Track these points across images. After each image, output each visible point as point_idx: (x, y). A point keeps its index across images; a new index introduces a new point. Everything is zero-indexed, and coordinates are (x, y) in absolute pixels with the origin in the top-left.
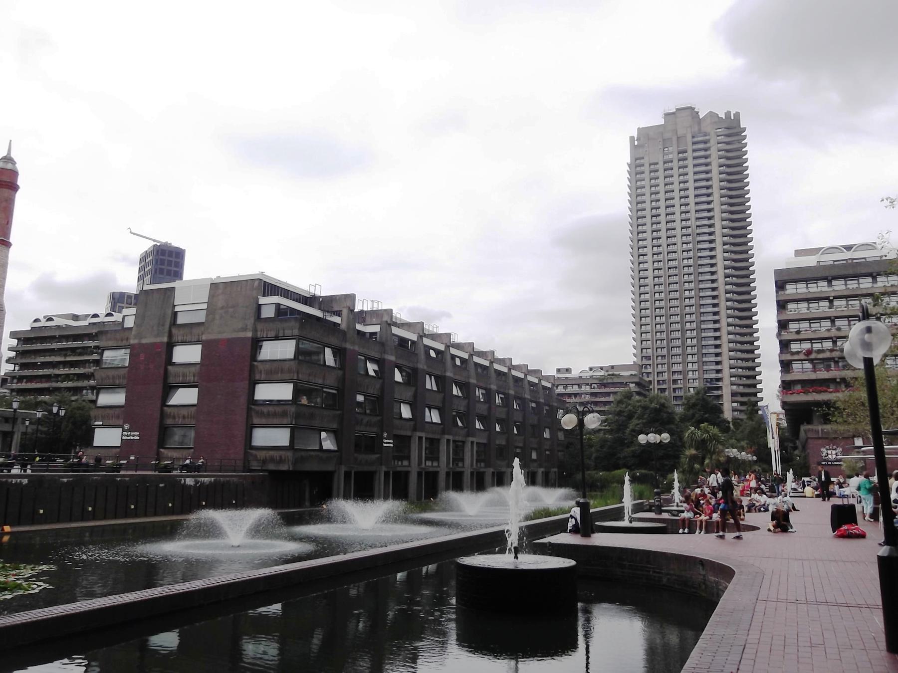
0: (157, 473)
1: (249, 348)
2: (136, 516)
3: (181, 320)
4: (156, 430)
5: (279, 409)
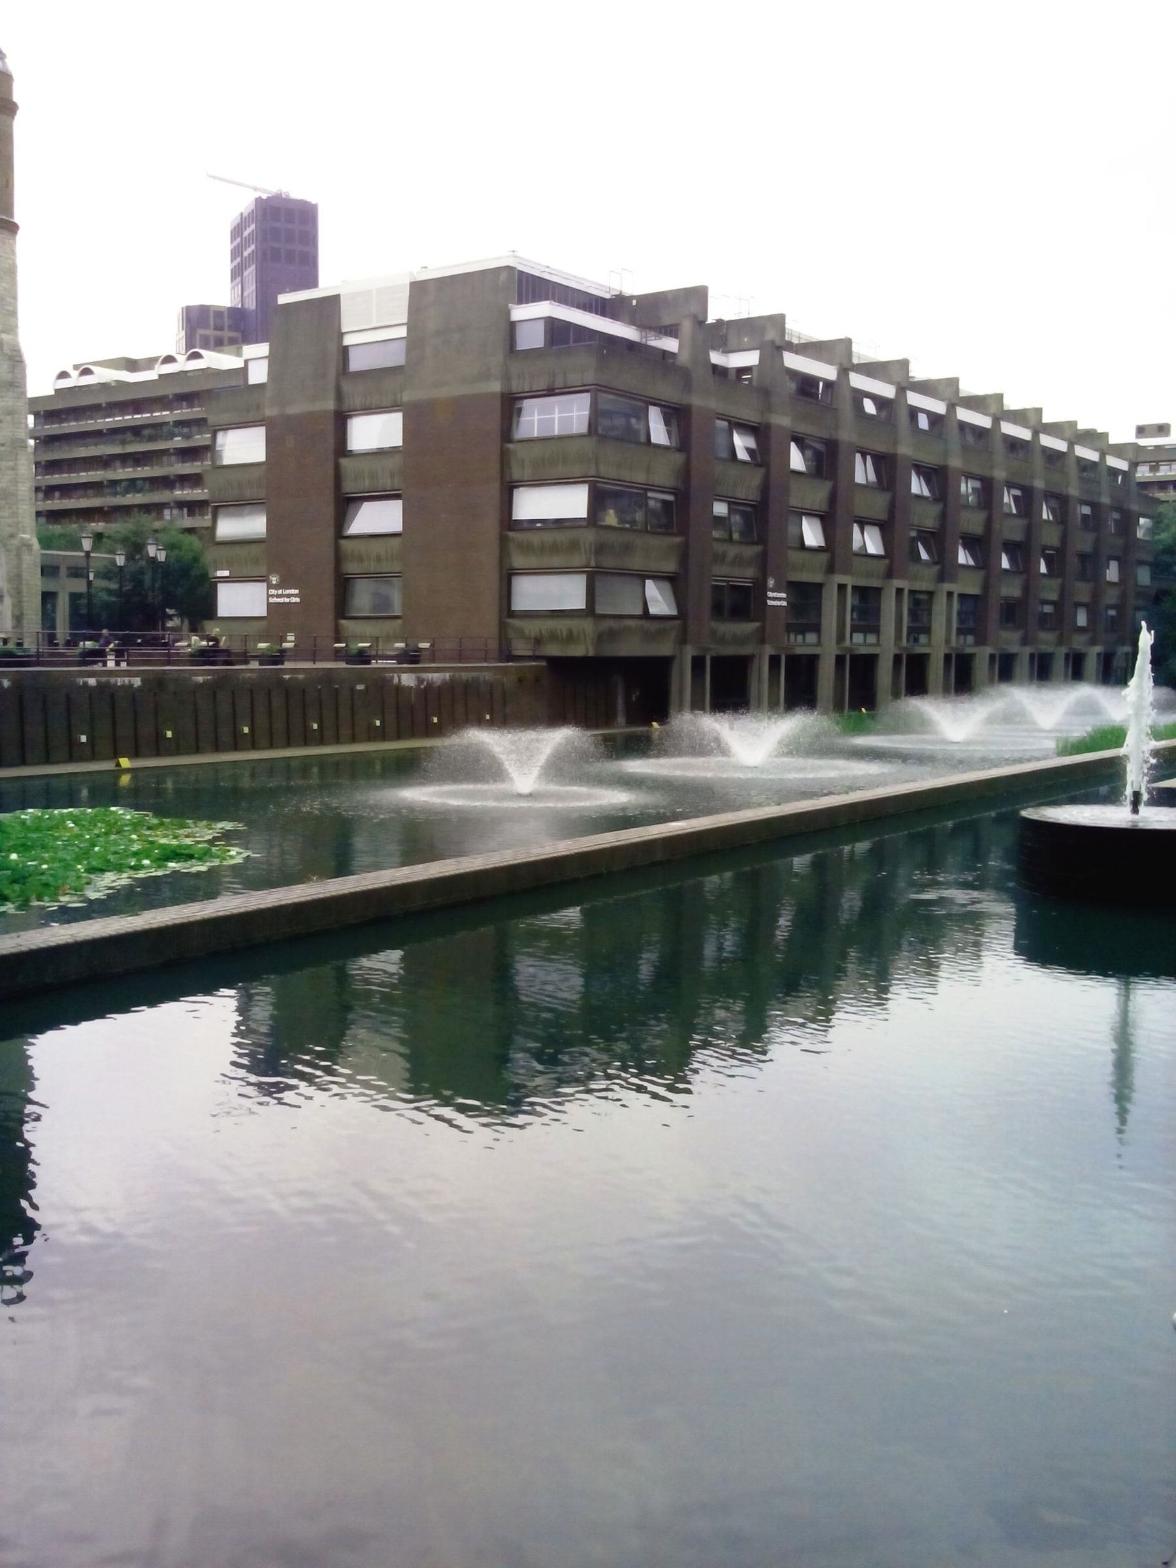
0: (342, 665)
1: (497, 415)
2: (322, 742)
3: (357, 363)
4: (329, 584)
5: (562, 537)
